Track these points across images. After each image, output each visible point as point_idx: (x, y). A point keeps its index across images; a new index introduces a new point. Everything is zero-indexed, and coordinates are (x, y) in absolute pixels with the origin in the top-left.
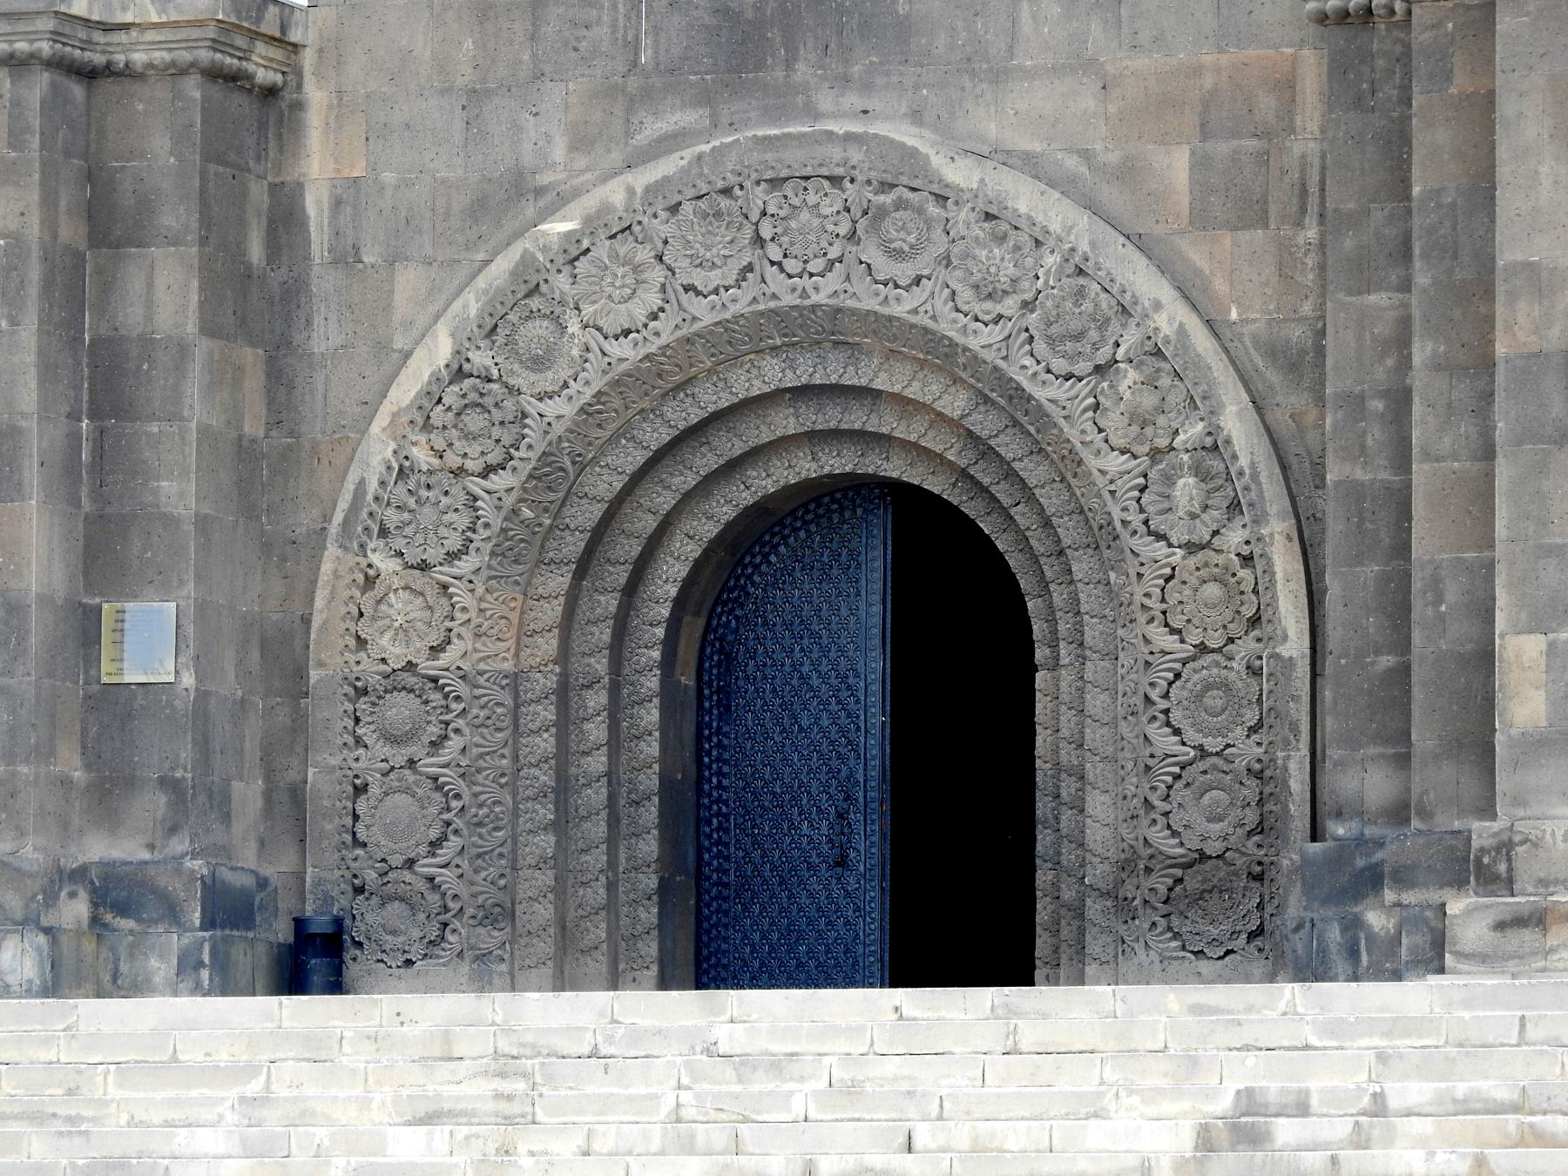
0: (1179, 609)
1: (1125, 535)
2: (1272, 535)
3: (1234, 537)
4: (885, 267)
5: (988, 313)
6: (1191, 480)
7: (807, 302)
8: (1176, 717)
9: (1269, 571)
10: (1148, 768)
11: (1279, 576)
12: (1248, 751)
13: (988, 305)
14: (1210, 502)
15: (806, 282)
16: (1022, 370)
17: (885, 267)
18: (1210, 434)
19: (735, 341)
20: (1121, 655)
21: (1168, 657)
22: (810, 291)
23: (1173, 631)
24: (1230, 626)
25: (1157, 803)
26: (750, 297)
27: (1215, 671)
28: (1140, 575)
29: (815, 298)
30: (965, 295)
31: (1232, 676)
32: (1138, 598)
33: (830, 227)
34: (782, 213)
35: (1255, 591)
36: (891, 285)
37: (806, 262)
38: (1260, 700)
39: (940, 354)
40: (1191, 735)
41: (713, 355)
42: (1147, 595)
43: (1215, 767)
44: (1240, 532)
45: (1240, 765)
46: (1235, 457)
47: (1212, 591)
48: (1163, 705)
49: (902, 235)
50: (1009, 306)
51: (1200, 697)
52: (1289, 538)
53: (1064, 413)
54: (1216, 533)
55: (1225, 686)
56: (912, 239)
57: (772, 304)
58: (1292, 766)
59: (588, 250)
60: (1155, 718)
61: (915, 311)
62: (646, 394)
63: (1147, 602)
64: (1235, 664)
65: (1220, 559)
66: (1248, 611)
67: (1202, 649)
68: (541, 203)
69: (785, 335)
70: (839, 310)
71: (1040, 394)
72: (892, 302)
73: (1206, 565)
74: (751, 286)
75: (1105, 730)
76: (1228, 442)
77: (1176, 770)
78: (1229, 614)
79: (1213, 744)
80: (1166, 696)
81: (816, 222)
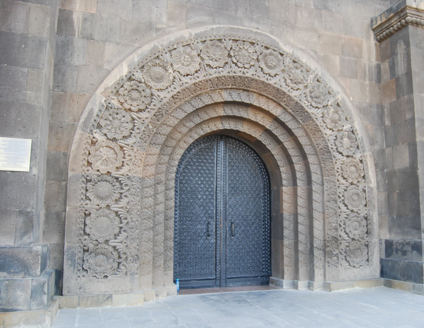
0: (346, 172)
1: (332, 152)
2: (367, 155)
3: (358, 156)
4: (266, 70)
5: (295, 87)
6: (347, 139)
7: (245, 76)
8: (346, 202)
9: (367, 164)
10: (340, 215)
11: (369, 166)
12: (363, 212)
13: (295, 85)
14: (352, 145)
15: (243, 70)
16: (305, 104)
17: (266, 70)
18: (351, 128)
19: (219, 84)
20: (326, 184)
21: (344, 185)
22: (245, 73)
23: (344, 178)
24: (358, 178)
25: (342, 225)
26: (227, 71)
27: (355, 190)
28: (336, 163)
29: (247, 75)
30: (288, 81)
31: (359, 192)
32: (336, 169)
33: (251, 56)
34: (237, 49)
35: (363, 170)
36: (268, 75)
37: (244, 64)
38: (366, 198)
39: (278, 96)
40: (350, 207)
41: (211, 87)
42: (338, 168)
43: (356, 216)
44: (360, 154)
45: (362, 215)
46: (358, 134)
47: (353, 168)
48: (343, 198)
49: (272, 62)
50: (301, 86)
51: (351, 196)
52: (371, 157)
53: (316, 117)
54: (354, 153)
55: (358, 195)
56: (274, 64)
57: (234, 74)
58: (374, 216)
59: (175, 49)
60: (341, 202)
61: (275, 83)
62: (190, 96)
63: (338, 170)
64: (359, 188)
65: (355, 161)
66: (362, 175)
67: (352, 184)
68: (158, 33)
69: (233, 85)
70: (253, 80)
71: (309, 111)
72: (269, 80)
73: (352, 162)
74: (227, 69)
75: (318, 204)
76: (356, 130)
77: (346, 216)
78: (357, 175)
79: (355, 210)
80: (343, 196)
81: (247, 54)
